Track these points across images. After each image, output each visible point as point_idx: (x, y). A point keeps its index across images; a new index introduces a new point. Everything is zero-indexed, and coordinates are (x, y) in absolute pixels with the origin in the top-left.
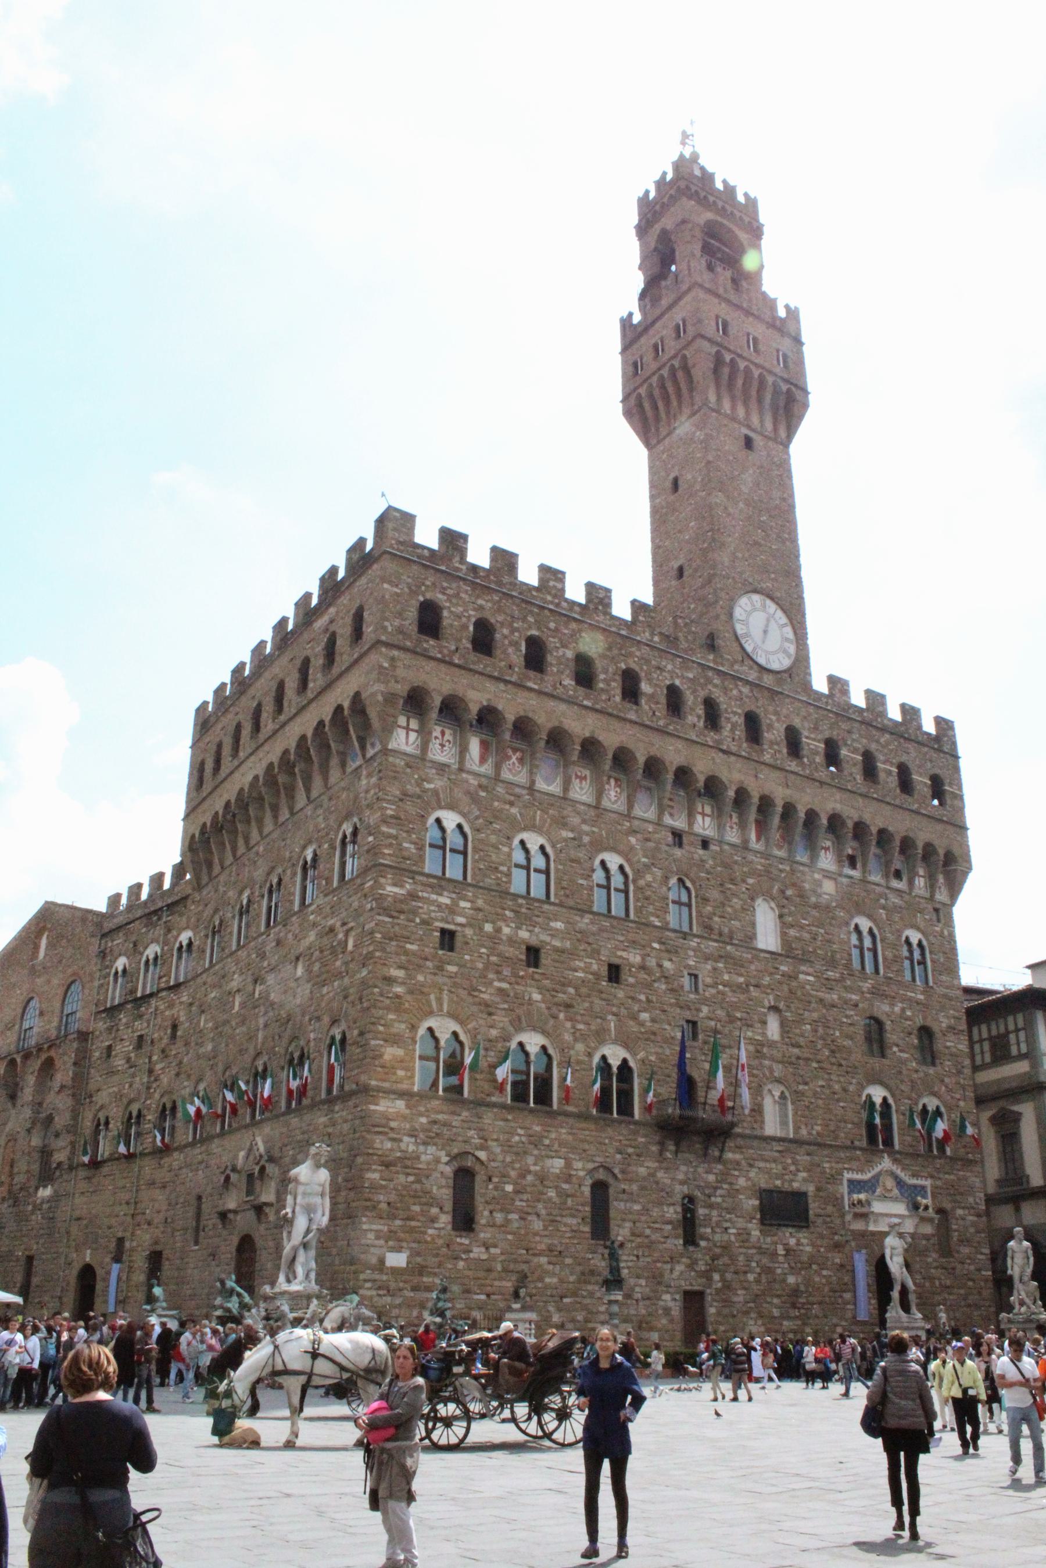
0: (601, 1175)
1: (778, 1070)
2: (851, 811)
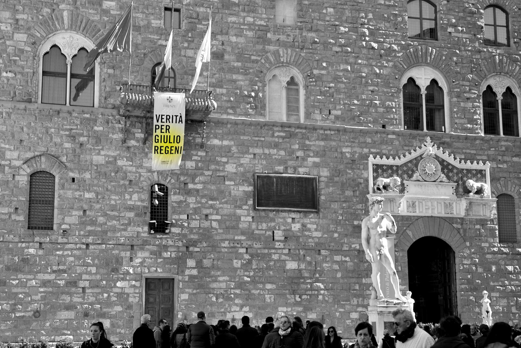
0: (44, 165)
1: (285, 54)
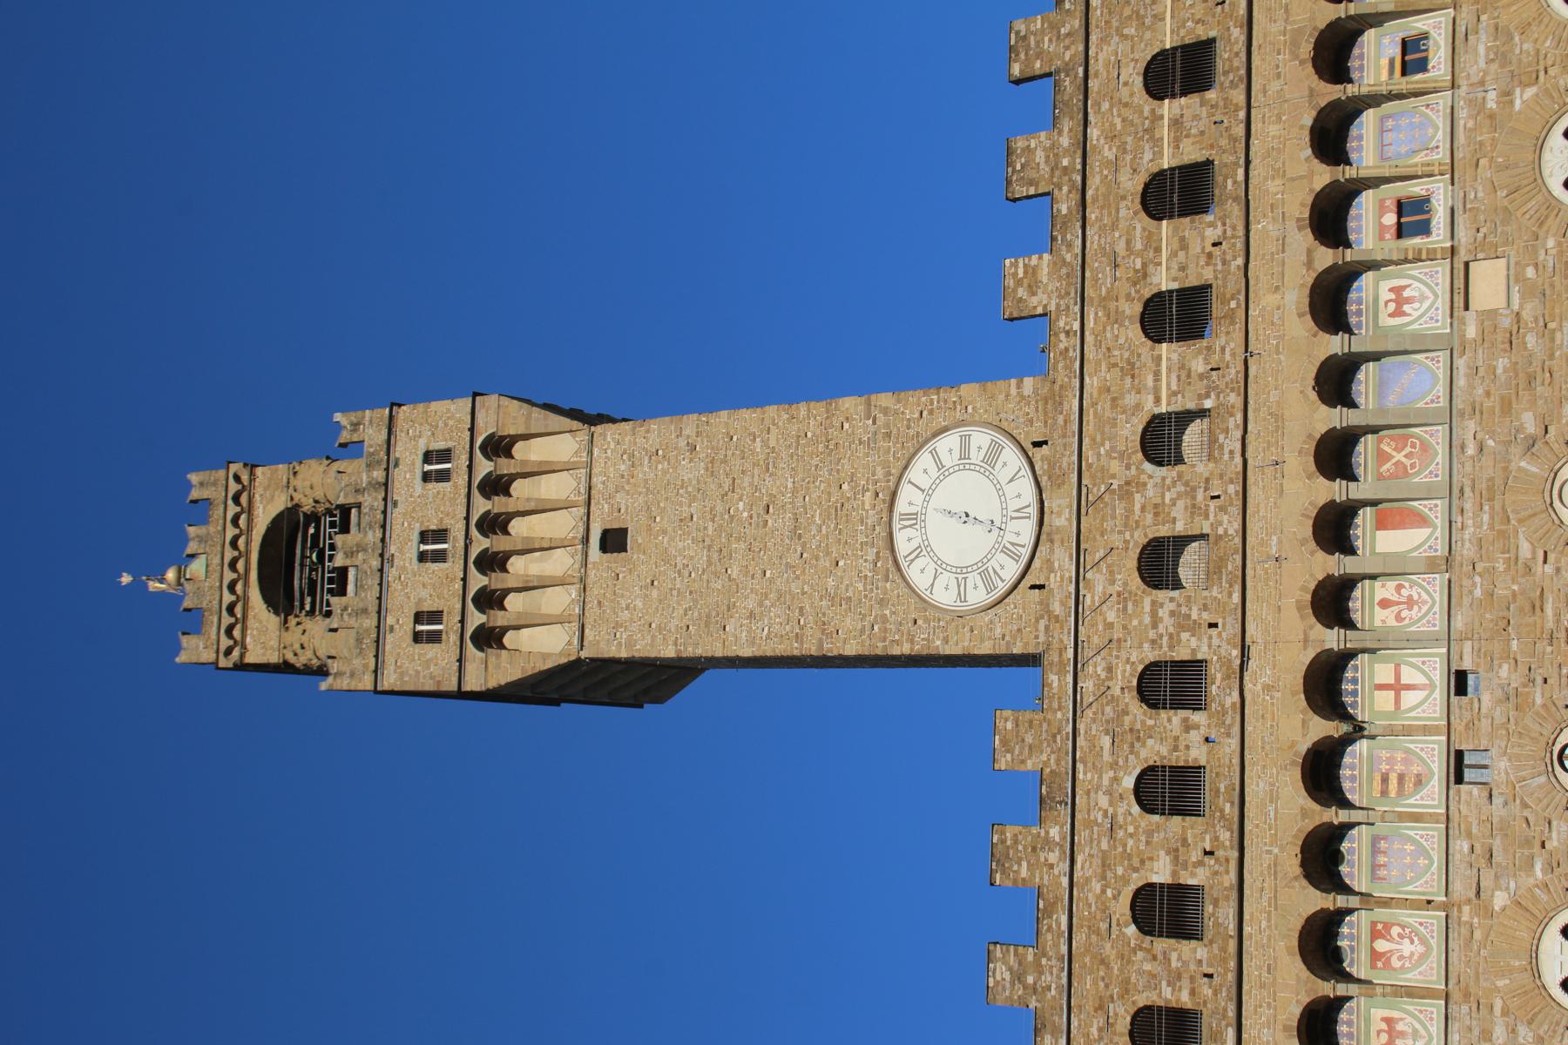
2: (1294, 259)
